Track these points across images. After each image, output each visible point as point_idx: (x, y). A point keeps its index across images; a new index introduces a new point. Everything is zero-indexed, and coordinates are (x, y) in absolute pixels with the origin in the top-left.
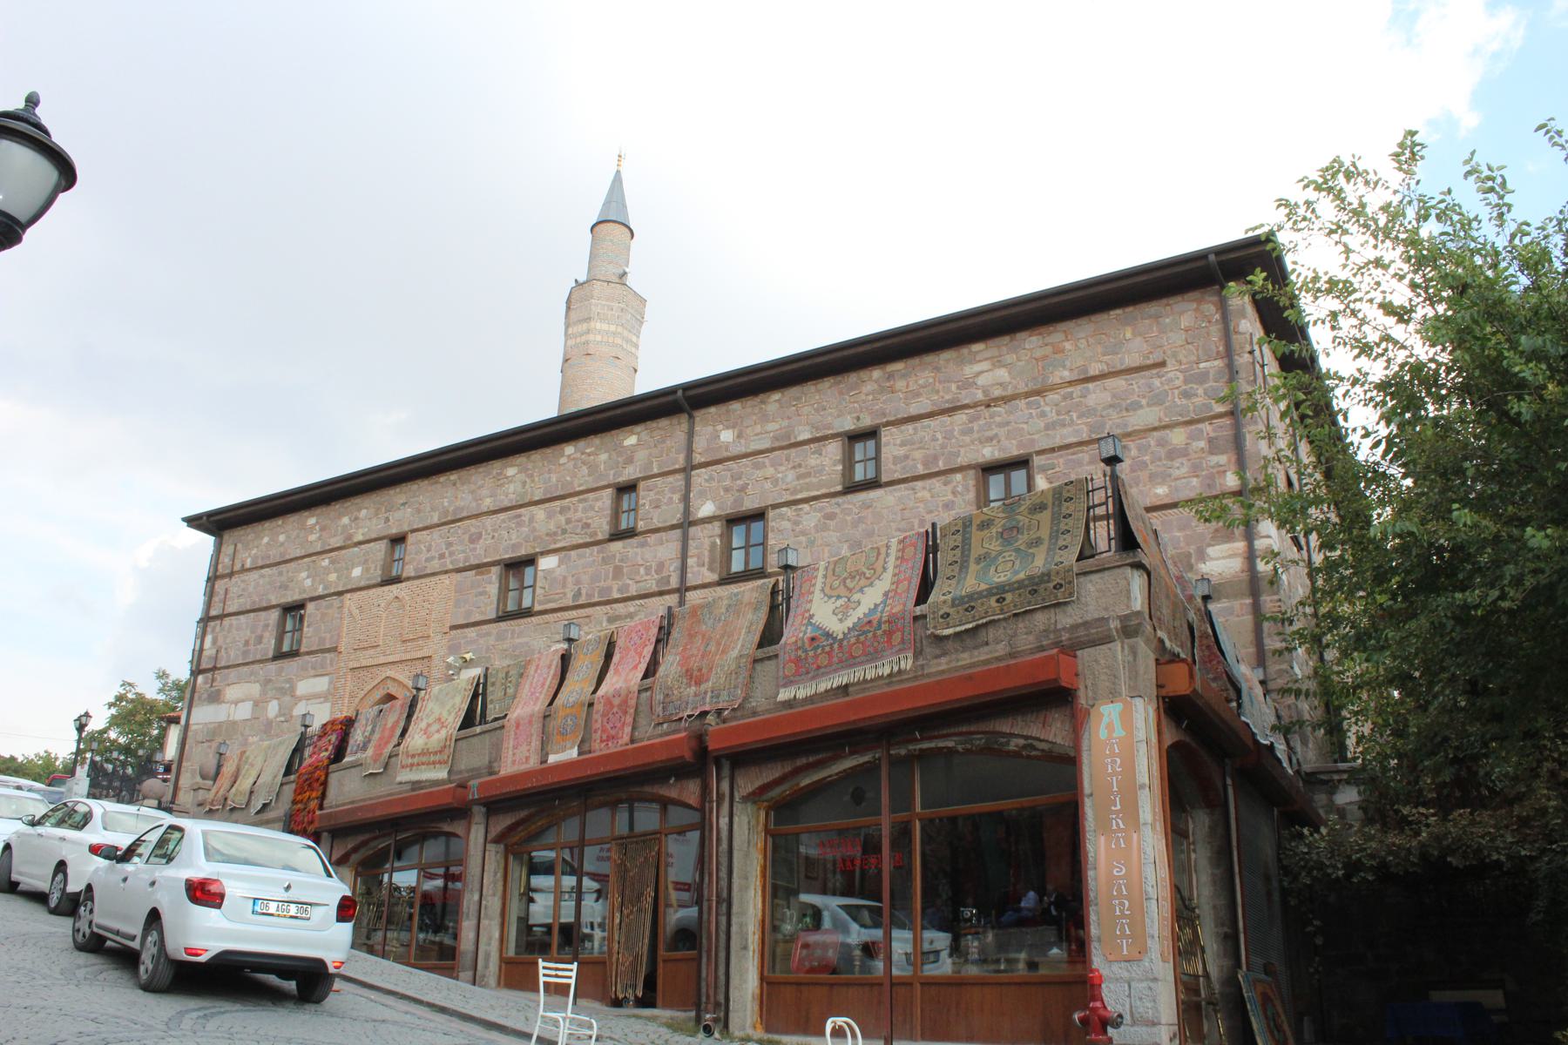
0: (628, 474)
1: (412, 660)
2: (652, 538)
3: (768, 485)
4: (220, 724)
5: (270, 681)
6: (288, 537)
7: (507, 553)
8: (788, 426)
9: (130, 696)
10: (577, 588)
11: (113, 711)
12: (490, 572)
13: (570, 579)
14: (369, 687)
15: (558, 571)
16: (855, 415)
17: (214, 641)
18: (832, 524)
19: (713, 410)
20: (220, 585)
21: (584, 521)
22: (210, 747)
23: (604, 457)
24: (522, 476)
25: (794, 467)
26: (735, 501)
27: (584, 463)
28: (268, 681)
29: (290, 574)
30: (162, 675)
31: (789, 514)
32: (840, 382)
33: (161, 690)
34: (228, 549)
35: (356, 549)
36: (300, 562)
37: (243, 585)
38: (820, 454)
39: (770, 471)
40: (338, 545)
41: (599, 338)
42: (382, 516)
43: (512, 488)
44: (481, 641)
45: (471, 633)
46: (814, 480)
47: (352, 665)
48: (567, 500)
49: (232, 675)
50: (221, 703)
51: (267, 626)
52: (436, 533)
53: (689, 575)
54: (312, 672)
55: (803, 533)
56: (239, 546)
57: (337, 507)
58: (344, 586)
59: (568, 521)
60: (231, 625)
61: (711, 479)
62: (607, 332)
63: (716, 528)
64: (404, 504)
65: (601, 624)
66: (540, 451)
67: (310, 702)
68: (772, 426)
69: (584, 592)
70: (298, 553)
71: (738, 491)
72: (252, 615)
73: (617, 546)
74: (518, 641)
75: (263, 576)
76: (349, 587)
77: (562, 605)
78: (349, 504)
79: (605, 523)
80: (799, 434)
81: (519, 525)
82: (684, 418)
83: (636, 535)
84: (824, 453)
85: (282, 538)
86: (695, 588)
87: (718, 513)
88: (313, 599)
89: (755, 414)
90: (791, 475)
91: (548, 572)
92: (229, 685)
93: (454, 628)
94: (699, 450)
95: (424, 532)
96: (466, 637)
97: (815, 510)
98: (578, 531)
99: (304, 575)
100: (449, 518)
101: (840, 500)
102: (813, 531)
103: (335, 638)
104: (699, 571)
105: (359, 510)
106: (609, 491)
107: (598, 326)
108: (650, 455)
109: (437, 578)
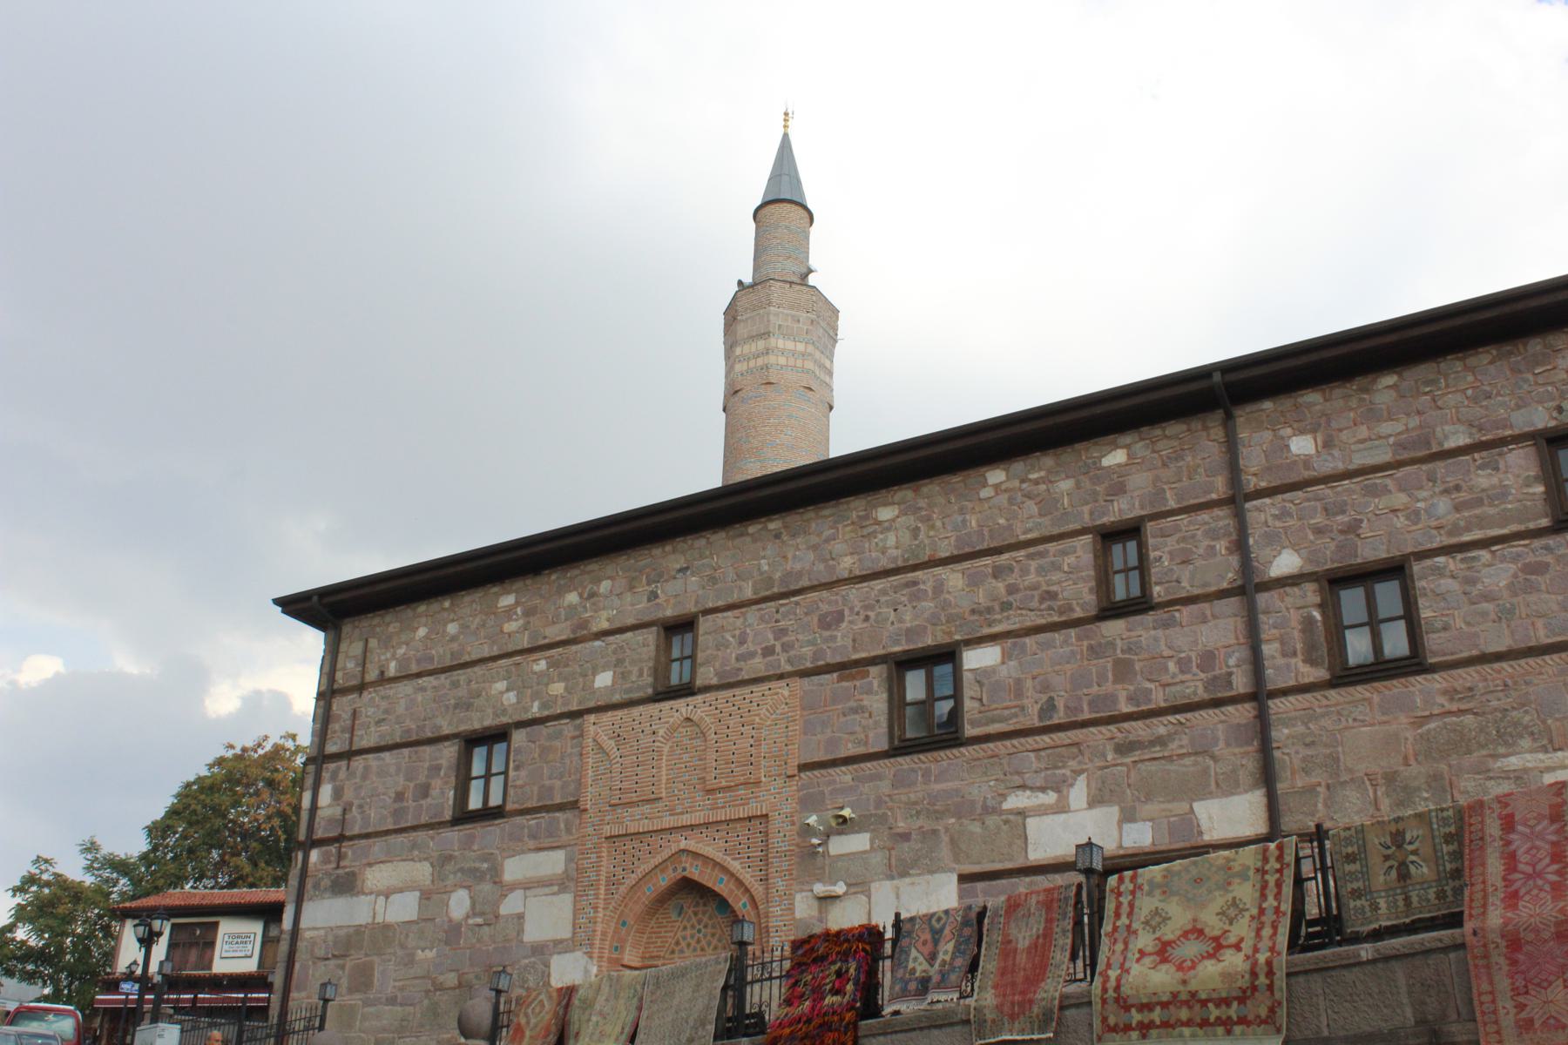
0: (1121, 510)
1: (728, 822)
2: (1184, 613)
3: (1400, 521)
4: (359, 930)
5: (450, 858)
6: (464, 627)
7: (897, 642)
8: (1421, 427)
9: (45, 877)
10: (1044, 698)
11: (19, 899)
12: (867, 674)
13: (1029, 683)
15: (1004, 671)
16: (1551, 404)
17: (337, 794)
18: (1542, 581)
19: (1267, 405)
20: (341, 706)
21: (1044, 588)
22: (343, 967)
23: (1065, 485)
24: (910, 520)
25: (1446, 491)
26: (1340, 548)
27: (1029, 496)
28: (447, 859)
29: (474, 686)
30: (91, 847)
31: (1452, 566)
32: (1511, 353)
33: (89, 869)
35: (597, 643)
36: (490, 665)
37: (384, 704)
38: (1497, 469)
39: (1400, 499)
40: (563, 637)
41: (782, 361)
42: (643, 588)
43: (891, 540)
45: (844, 775)
46: (1491, 511)
47: (607, 830)
48: (1006, 556)
49: (376, 849)
50: (357, 894)
52: (752, 614)
53: (1269, 672)
54: (532, 844)
55: (1487, 597)
56: (373, 643)
57: (554, 577)
58: (580, 703)
59: (1012, 590)
60: (367, 768)
61: (1284, 514)
62: (794, 353)
63: (1310, 594)
64: (683, 570)
65: (1104, 756)
66: (937, 480)
67: (528, 893)
68: (1386, 428)
69: (1060, 704)
70: (486, 652)
71: (1341, 532)
72: (406, 751)
73: (1114, 628)
74: (938, 787)
75: (423, 689)
76: (591, 704)
77: (1018, 727)
78: (576, 572)
79: (1086, 590)
80: (1446, 437)
81: (915, 597)
82: (1215, 420)
83: (1152, 608)
84: (1502, 465)
85: (452, 628)
86: (1285, 692)
87: (1309, 569)
88: (521, 725)
89: (1351, 409)
90: (1443, 505)
91: (982, 675)
92: (370, 865)
93: (804, 767)
94: (1253, 470)
95: (729, 614)
96: (834, 781)
97: (1503, 560)
98: (1035, 604)
99: (501, 686)
100: (776, 590)
101: (1551, 541)
102: (1506, 594)
103: (572, 787)
104: (1288, 666)
105: (598, 581)
106: (1088, 538)
107: (781, 343)
108: (1157, 479)
109: (764, 687)
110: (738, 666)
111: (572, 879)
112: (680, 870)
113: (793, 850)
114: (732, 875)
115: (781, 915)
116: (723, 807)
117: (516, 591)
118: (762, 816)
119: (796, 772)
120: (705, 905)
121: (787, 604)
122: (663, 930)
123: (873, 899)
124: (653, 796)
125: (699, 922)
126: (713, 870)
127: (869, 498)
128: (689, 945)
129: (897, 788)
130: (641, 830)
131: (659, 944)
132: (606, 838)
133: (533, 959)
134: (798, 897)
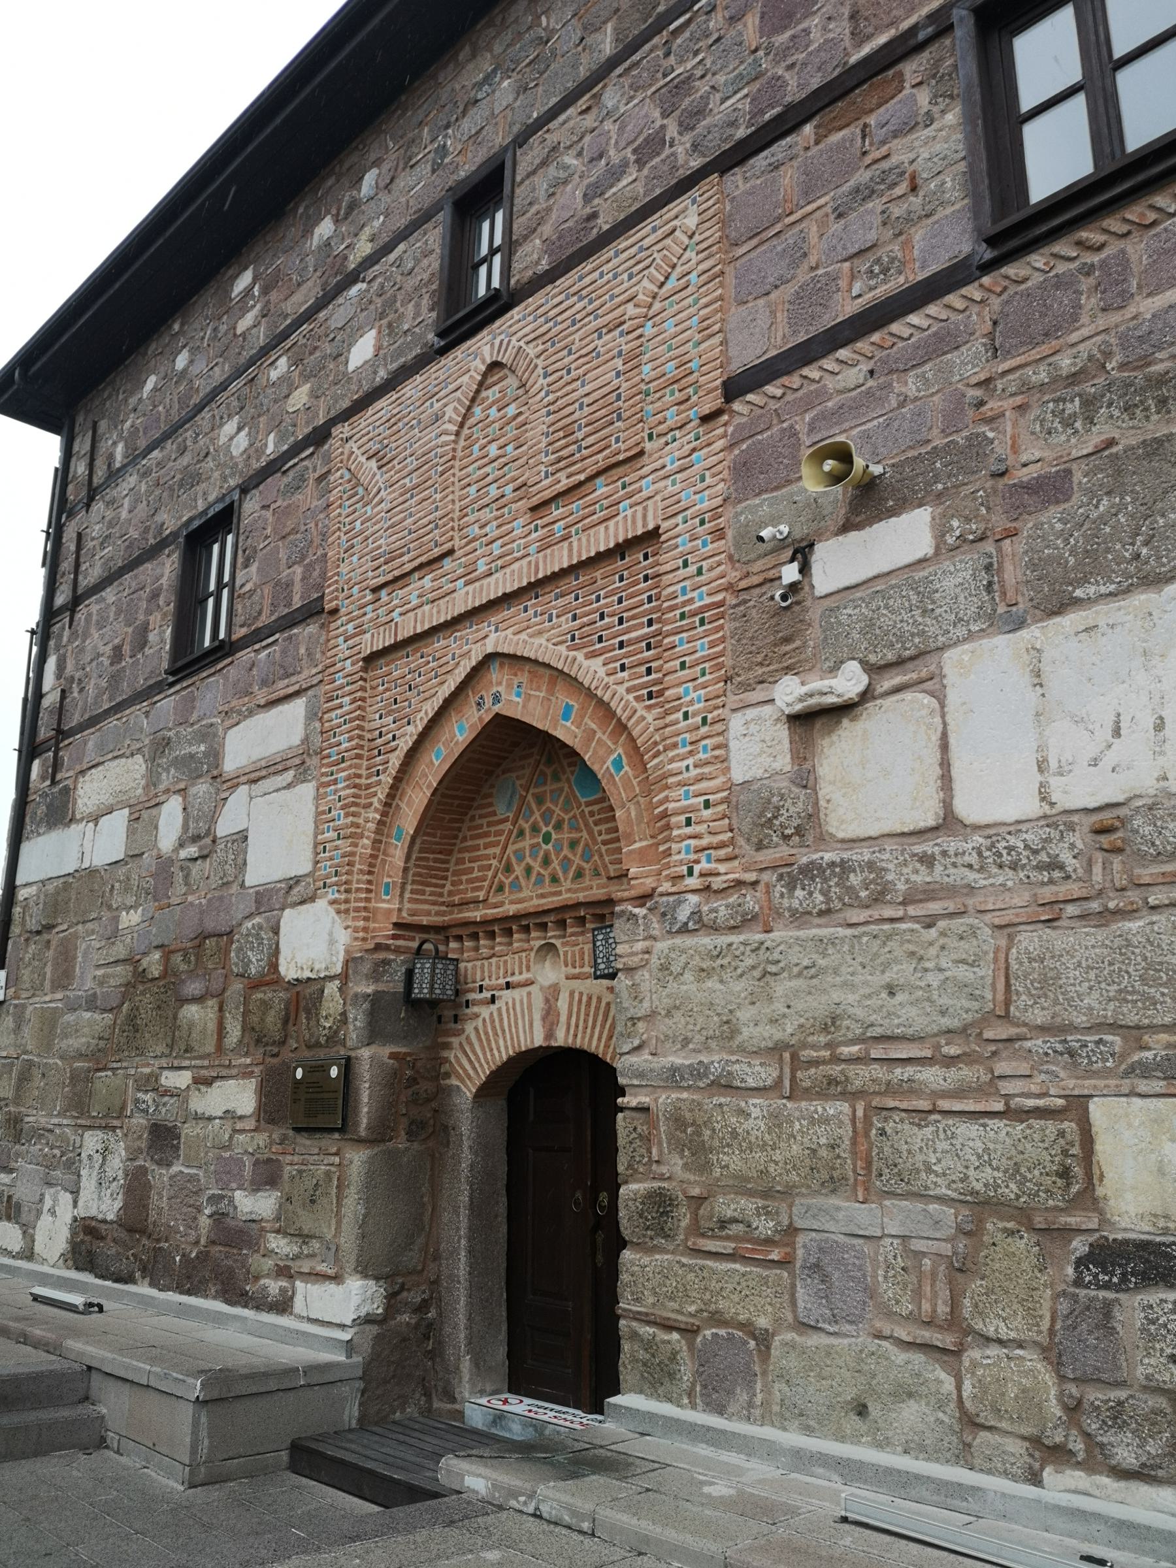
14: (430, 708)
17: (61, 667)
28: (161, 745)
34: (82, 445)
44: (911, 385)
51: (155, 595)
74: (1148, 306)
92: (82, 772)
93: (733, 389)
96: (822, 395)
99: (230, 427)
110: (588, 210)
112: (488, 701)
114: (589, 694)
115: (700, 779)
116: (565, 539)
120: (556, 778)
121: (689, 21)
122: (481, 842)
123: (952, 697)
125: (547, 816)
126: (551, 691)
128: (528, 870)
129: (1008, 354)
133: (257, 920)
134: (736, 723)
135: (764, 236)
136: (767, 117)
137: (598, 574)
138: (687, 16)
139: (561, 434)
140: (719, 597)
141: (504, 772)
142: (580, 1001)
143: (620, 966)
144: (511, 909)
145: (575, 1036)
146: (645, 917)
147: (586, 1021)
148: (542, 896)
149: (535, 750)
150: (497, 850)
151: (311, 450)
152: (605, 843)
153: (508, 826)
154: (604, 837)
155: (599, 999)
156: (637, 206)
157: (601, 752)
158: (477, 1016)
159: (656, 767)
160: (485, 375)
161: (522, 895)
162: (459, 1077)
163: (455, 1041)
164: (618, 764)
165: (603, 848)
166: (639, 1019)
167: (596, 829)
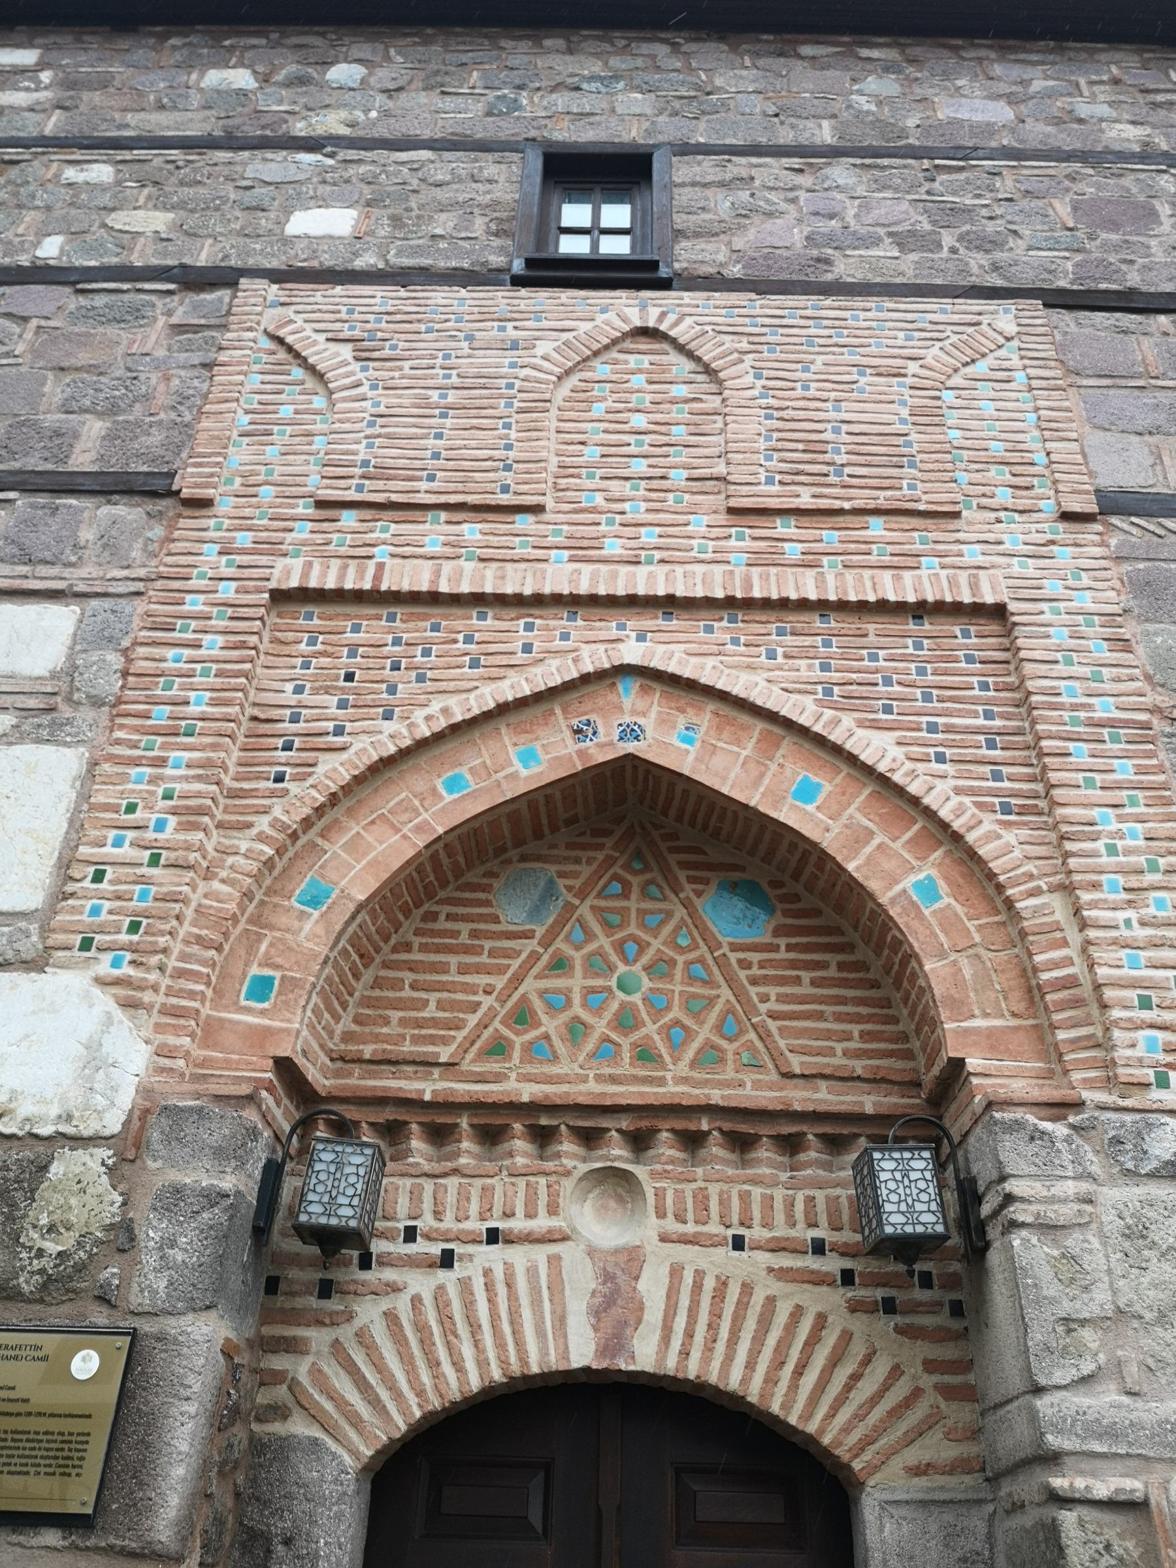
111: (97, 702)
113: (1147, 726)
117: (46, 48)
118: (978, 611)
119: (1095, 508)
122: (453, 960)
124: (505, 499)
127: (1147, 55)
128: (576, 1030)
130: (444, 588)
131: (430, 1012)
132: (280, 597)
135: (1123, 382)
136: (1103, 286)
137: (871, 628)
138: (961, 163)
139: (801, 446)
140: (1143, 717)
141: (523, 858)
142: (698, 1287)
143: (1029, 1219)
144: (527, 1092)
145: (685, 1354)
146: (1068, 1140)
147: (712, 1327)
148: (614, 1079)
149: (609, 842)
150: (500, 982)
151: (172, 286)
152: (773, 1015)
153: (532, 945)
154: (772, 1005)
155: (747, 1289)
156: (898, 280)
157: (888, 865)
158: (395, 1289)
159: (1036, 910)
160: (625, 335)
161: (555, 1070)
162: (316, 1417)
163: (318, 1337)
164: (928, 889)
165: (772, 1025)
166: (1083, 1322)
167: (753, 991)
